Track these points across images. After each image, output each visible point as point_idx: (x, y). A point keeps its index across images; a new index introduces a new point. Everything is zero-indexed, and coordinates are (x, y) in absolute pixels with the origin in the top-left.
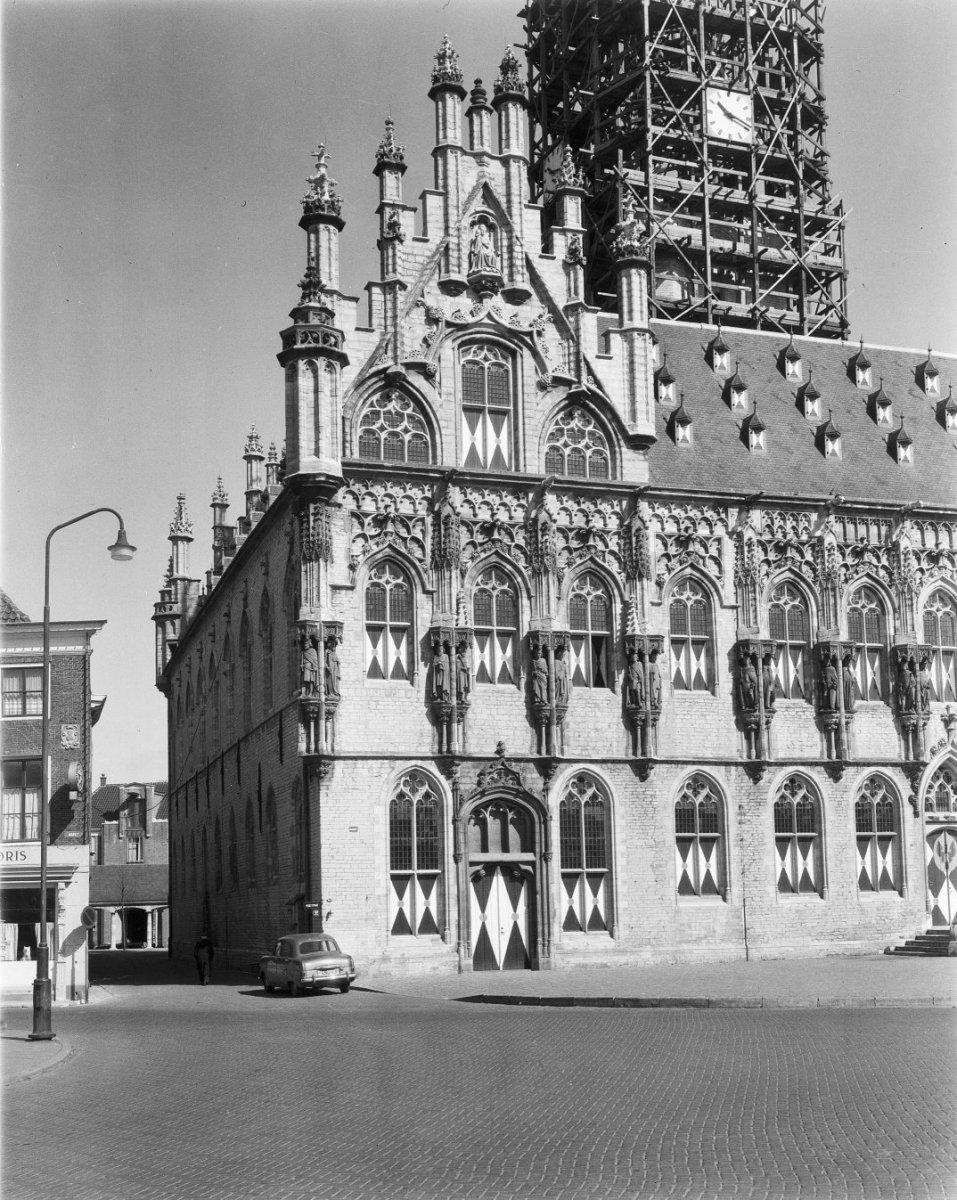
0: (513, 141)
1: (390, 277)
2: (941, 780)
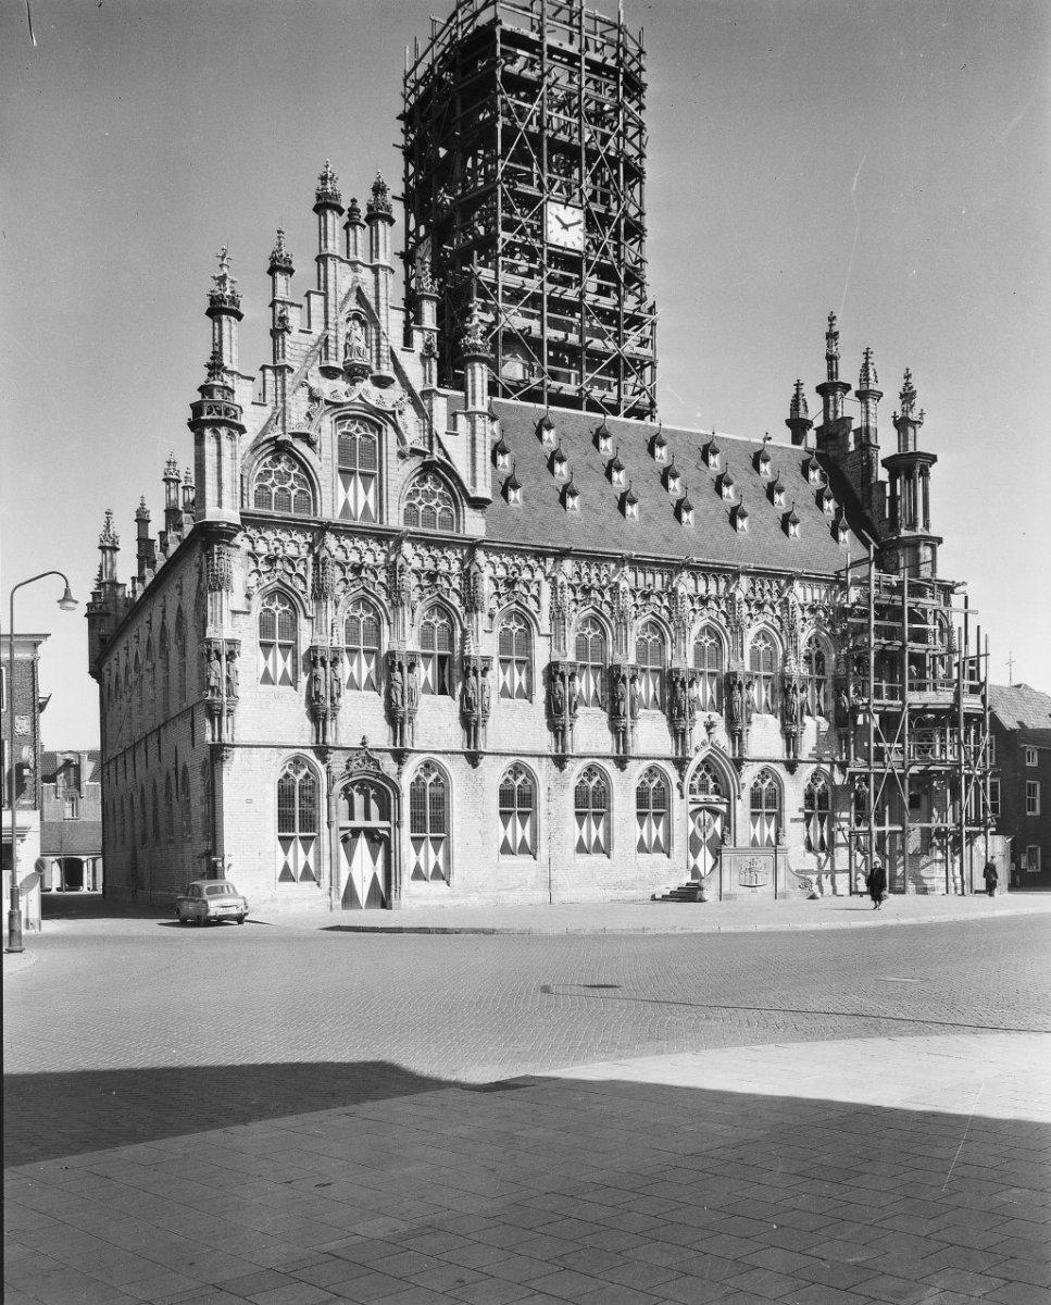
0: (381, 253)
1: (280, 362)
2: (703, 771)
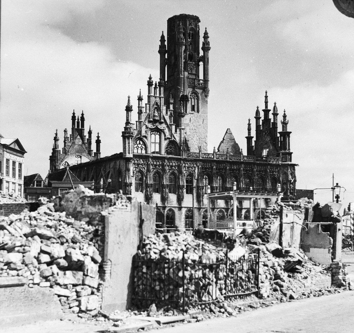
1: (140, 120)
